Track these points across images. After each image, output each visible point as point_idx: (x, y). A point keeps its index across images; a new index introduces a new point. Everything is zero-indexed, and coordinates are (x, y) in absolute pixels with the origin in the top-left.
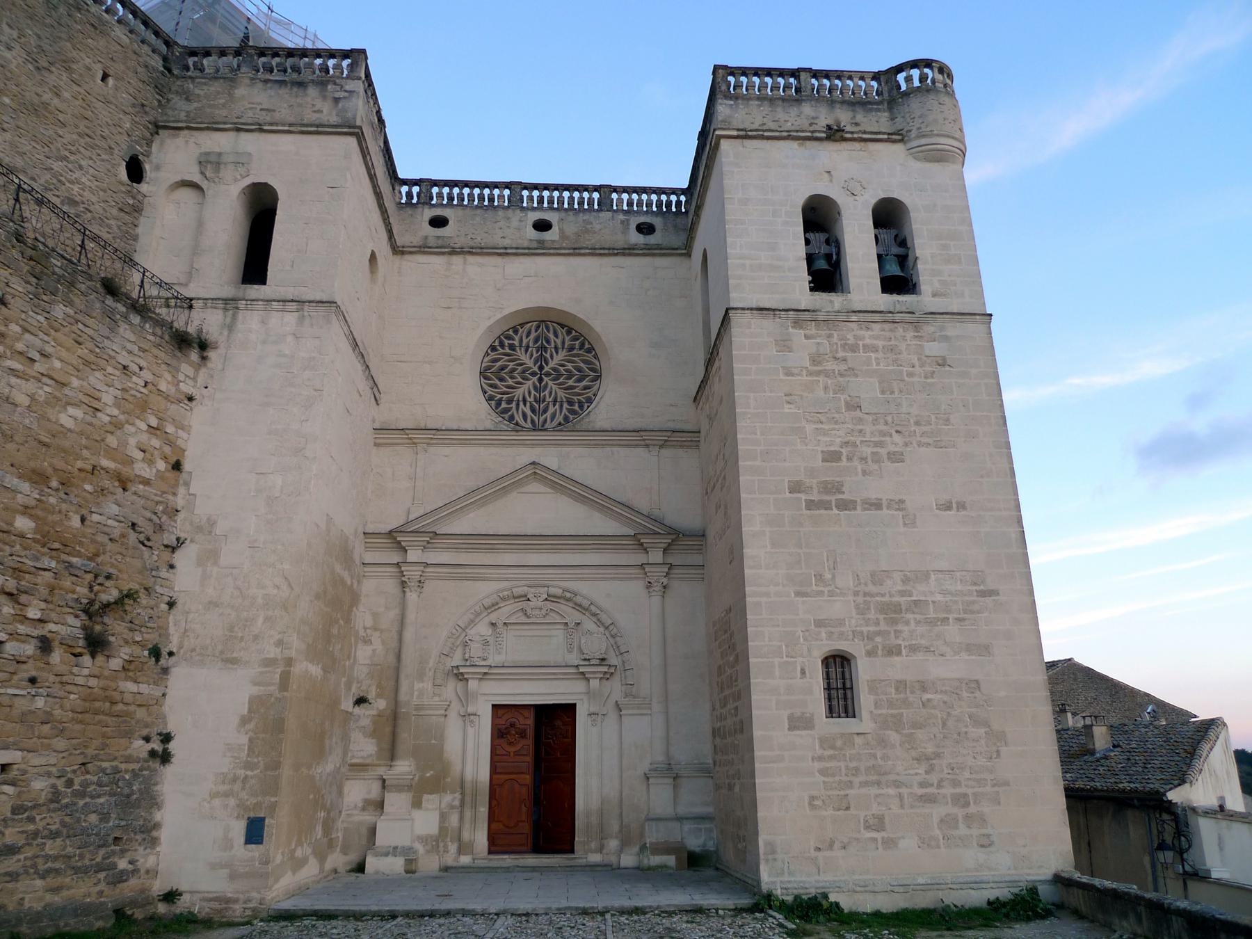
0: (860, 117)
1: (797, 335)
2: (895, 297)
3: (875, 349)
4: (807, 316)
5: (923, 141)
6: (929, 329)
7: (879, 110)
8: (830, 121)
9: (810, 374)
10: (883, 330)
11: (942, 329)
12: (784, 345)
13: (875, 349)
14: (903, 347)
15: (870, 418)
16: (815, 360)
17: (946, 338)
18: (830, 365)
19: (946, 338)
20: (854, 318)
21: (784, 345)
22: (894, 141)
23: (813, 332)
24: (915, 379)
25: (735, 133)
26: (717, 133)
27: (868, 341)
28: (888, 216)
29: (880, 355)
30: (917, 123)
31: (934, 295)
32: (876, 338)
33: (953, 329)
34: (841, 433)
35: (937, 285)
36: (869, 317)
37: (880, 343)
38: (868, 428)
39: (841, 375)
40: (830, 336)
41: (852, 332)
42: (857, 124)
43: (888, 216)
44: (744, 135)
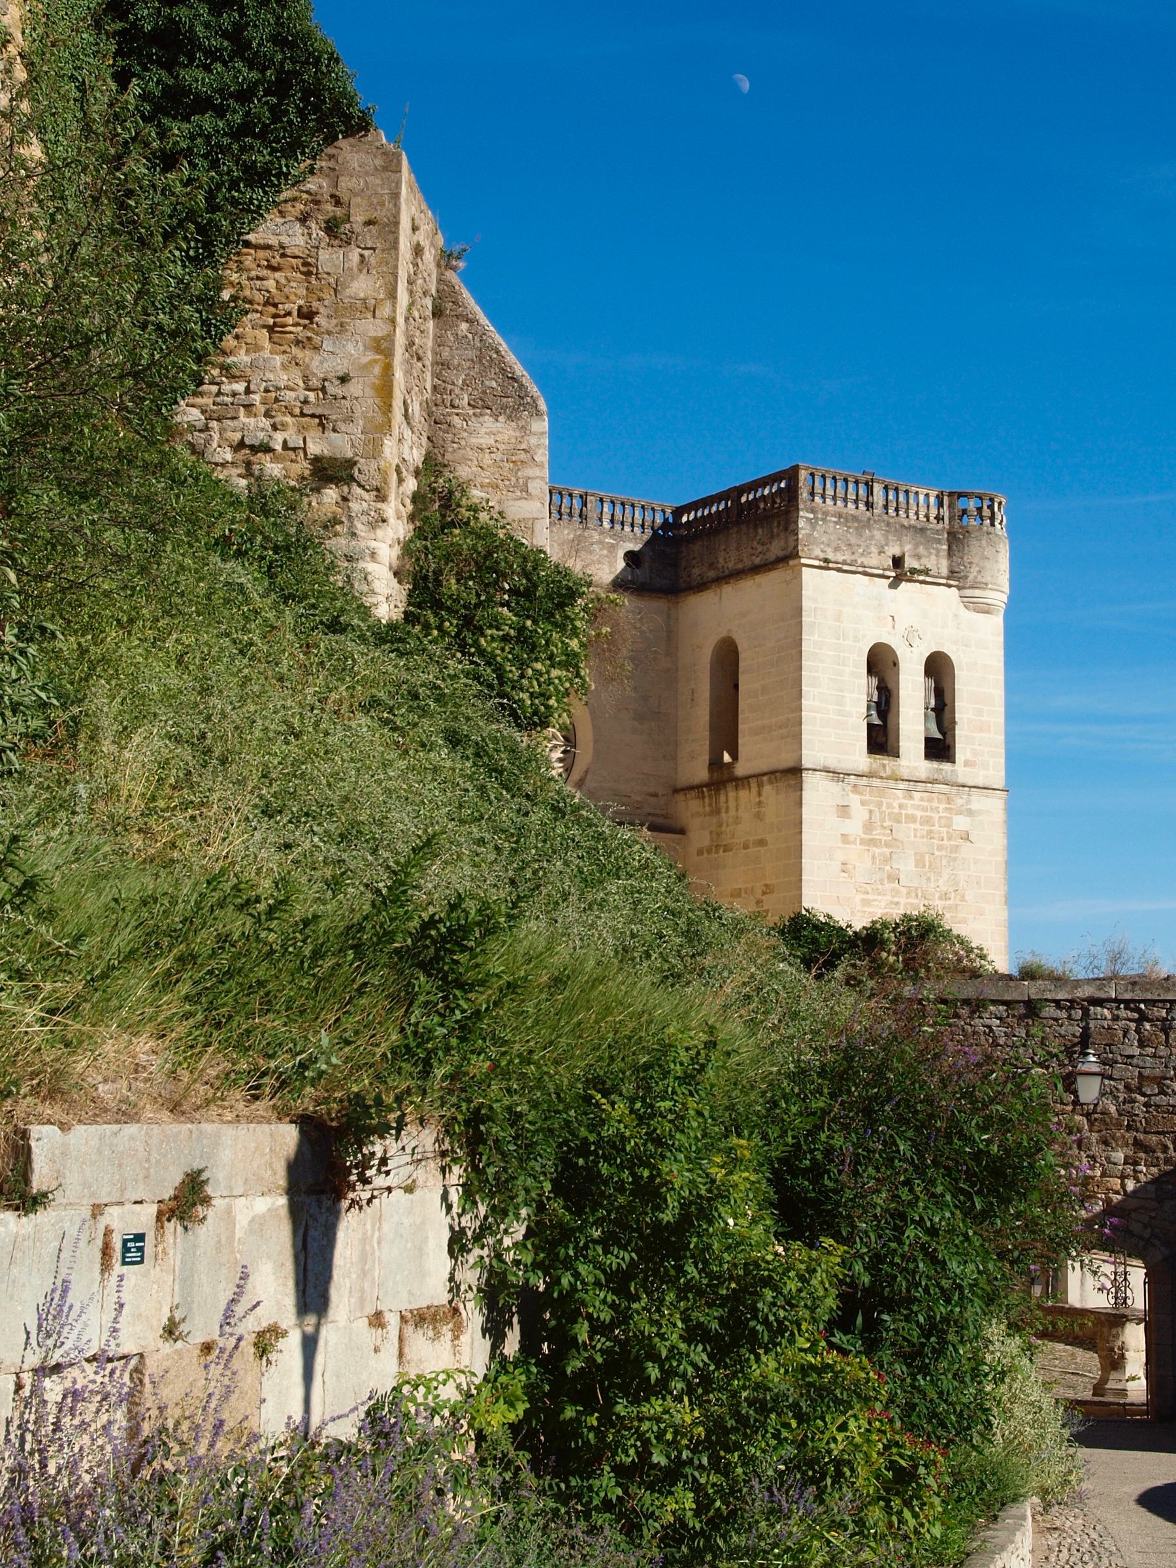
0: (921, 549)
1: (854, 800)
2: (935, 765)
3: (911, 819)
4: (864, 781)
5: (977, 593)
6: (960, 802)
7: (939, 541)
8: (898, 553)
9: (862, 842)
10: (922, 799)
11: (968, 802)
12: (844, 810)
13: (911, 819)
14: (936, 816)
15: (904, 891)
16: (869, 826)
17: (970, 813)
18: (877, 834)
19: (970, 813)
20: (902, 785)
21: (844, 810)
22: (950, 586)
23: (867, 797)
24: (943, 853)
25: (816, 563)
26: (803, 561)
27: (910, 811)
28: (938, 668)
29: (918, 826)
30: (974, 570)
31: (967, 763)
32: (917, 807)
33: (979, 802)
34: (883, 904)
35: (969, 756)
36: (911, 786)
37: (919, 813)
38: (903, 901)
39: (887, 845)
40: (880, 805)
41: (897, 796)
42: (918, 557)
43: (938, 668)
44: (826, 565)
